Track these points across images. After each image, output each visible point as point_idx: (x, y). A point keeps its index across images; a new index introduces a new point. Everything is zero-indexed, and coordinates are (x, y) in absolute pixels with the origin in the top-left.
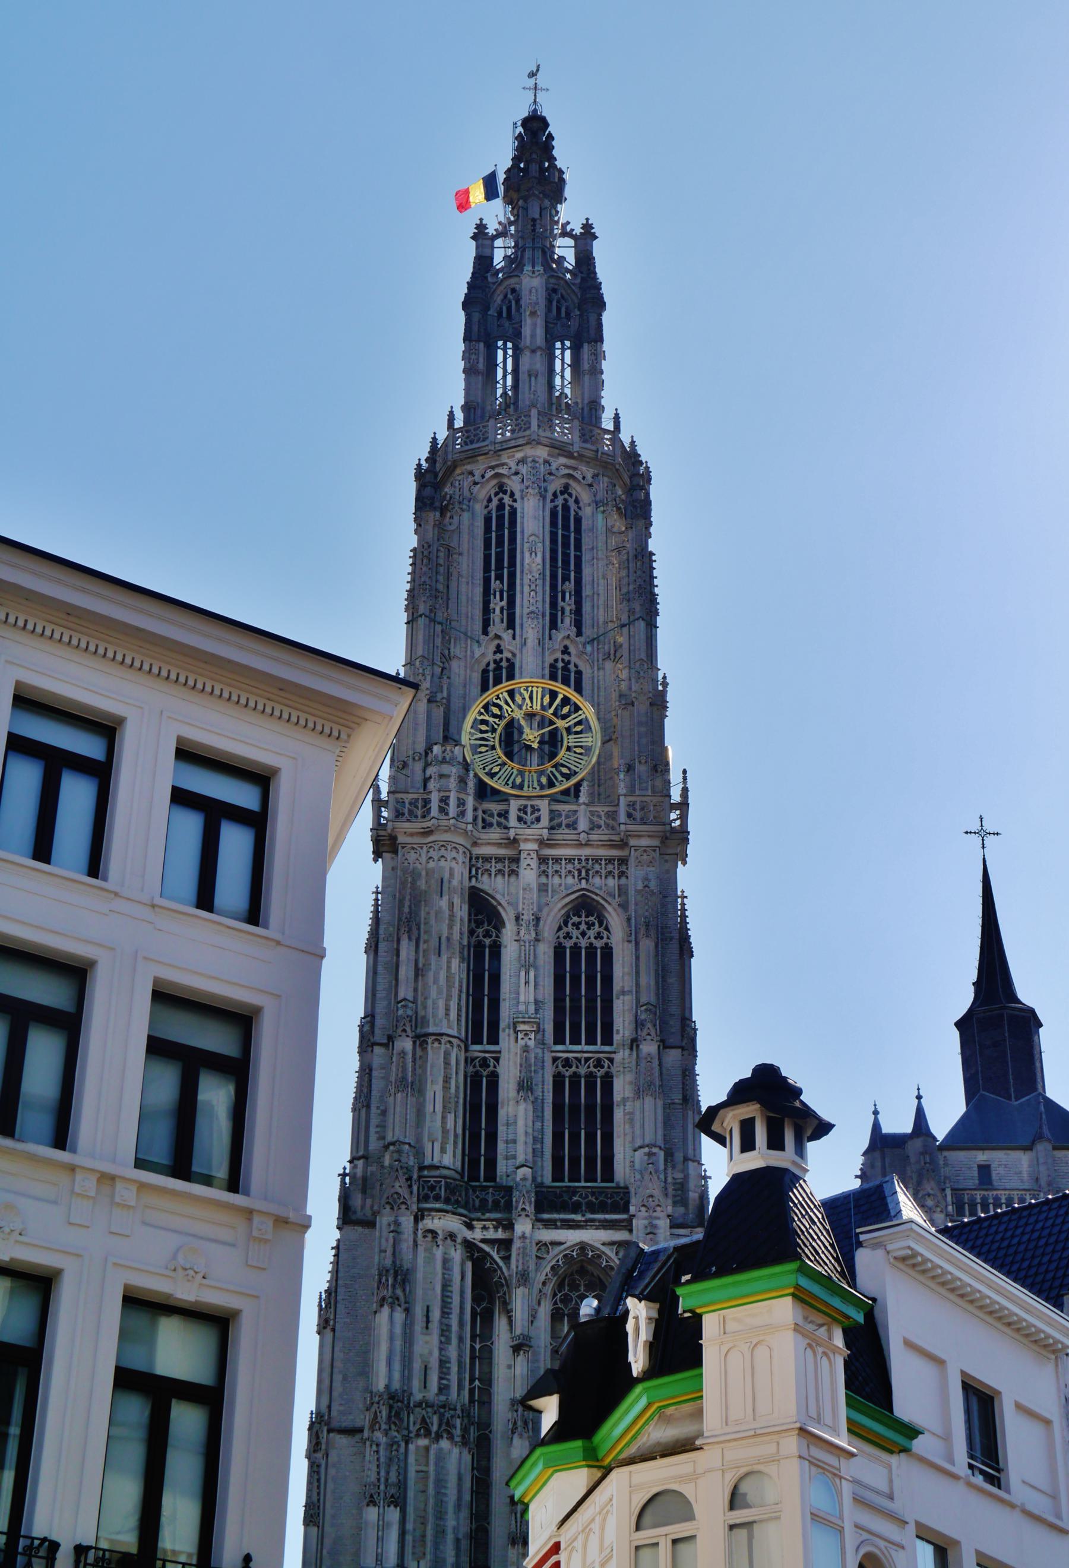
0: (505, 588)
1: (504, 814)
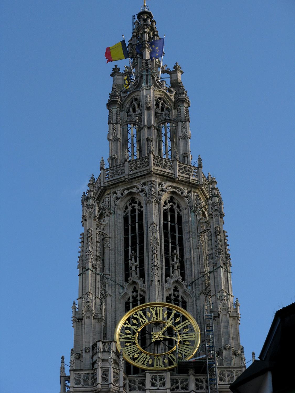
0: (138, 255)
1: (143, 383)
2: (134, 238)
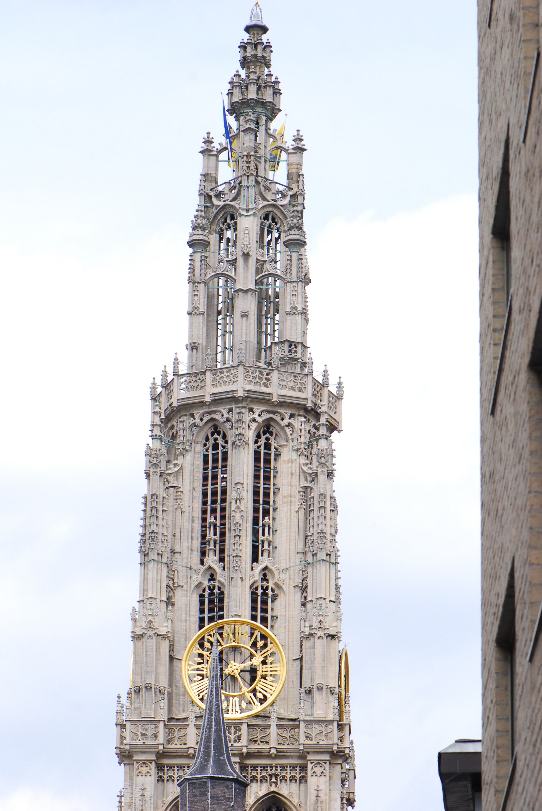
0: (218, 524)
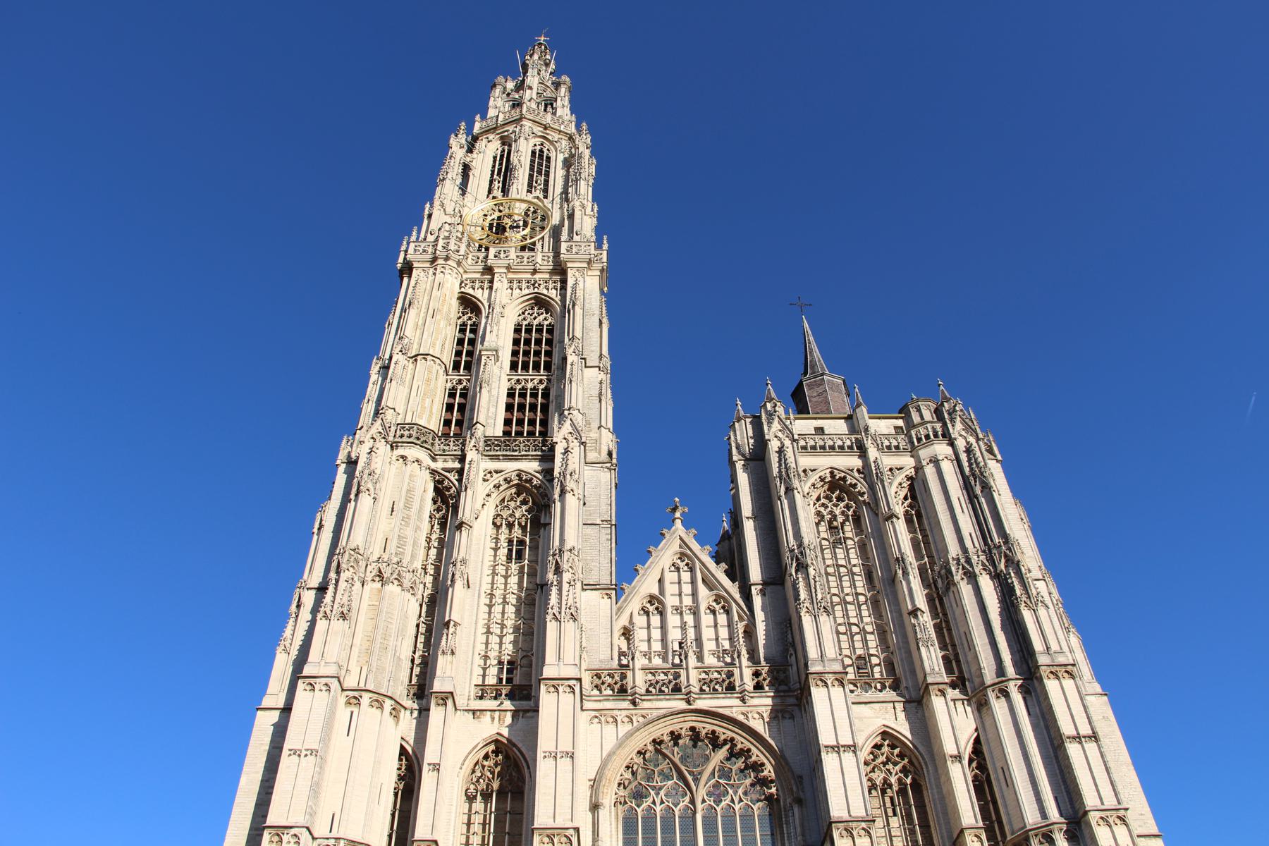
2: (500, 170)
